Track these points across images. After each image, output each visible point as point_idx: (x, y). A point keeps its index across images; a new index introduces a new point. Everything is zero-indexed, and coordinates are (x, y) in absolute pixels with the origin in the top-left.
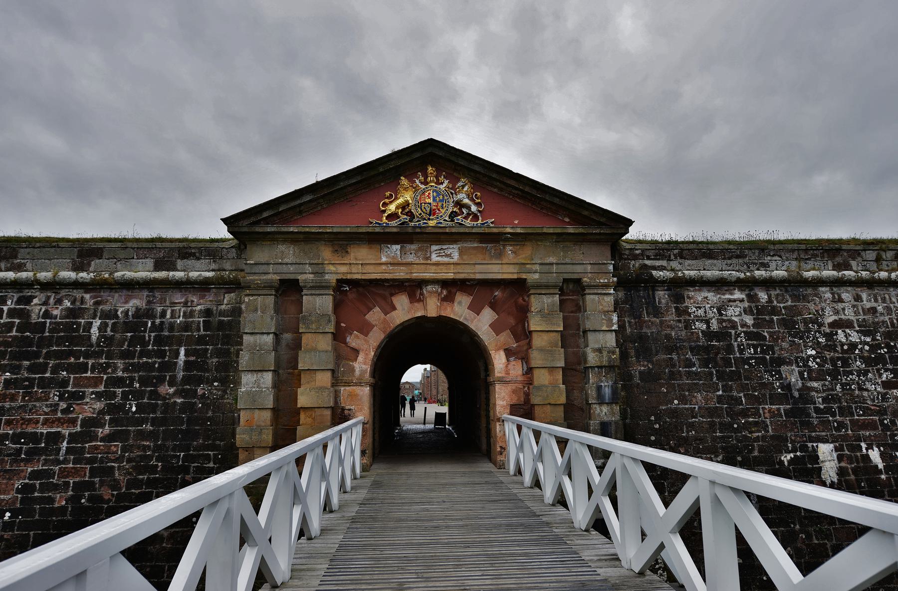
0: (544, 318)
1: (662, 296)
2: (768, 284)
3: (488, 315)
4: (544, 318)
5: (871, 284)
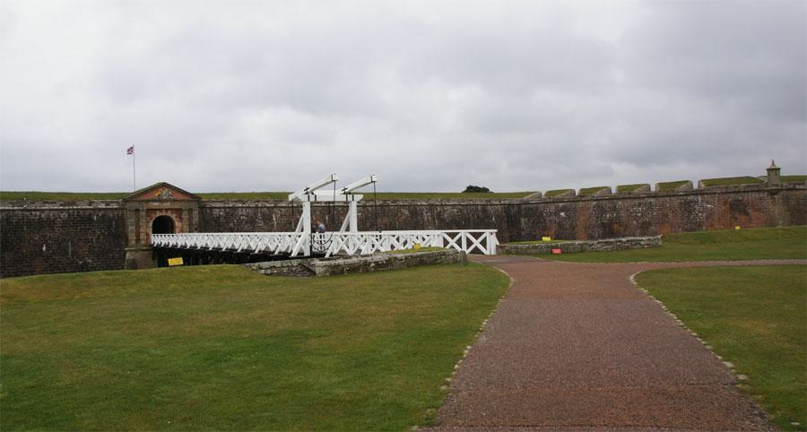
0: (185, 215)
1: (208, 211)
2: (229, 208)
3: (175, 215)
4: (185, 215)
5: (249, 207)
